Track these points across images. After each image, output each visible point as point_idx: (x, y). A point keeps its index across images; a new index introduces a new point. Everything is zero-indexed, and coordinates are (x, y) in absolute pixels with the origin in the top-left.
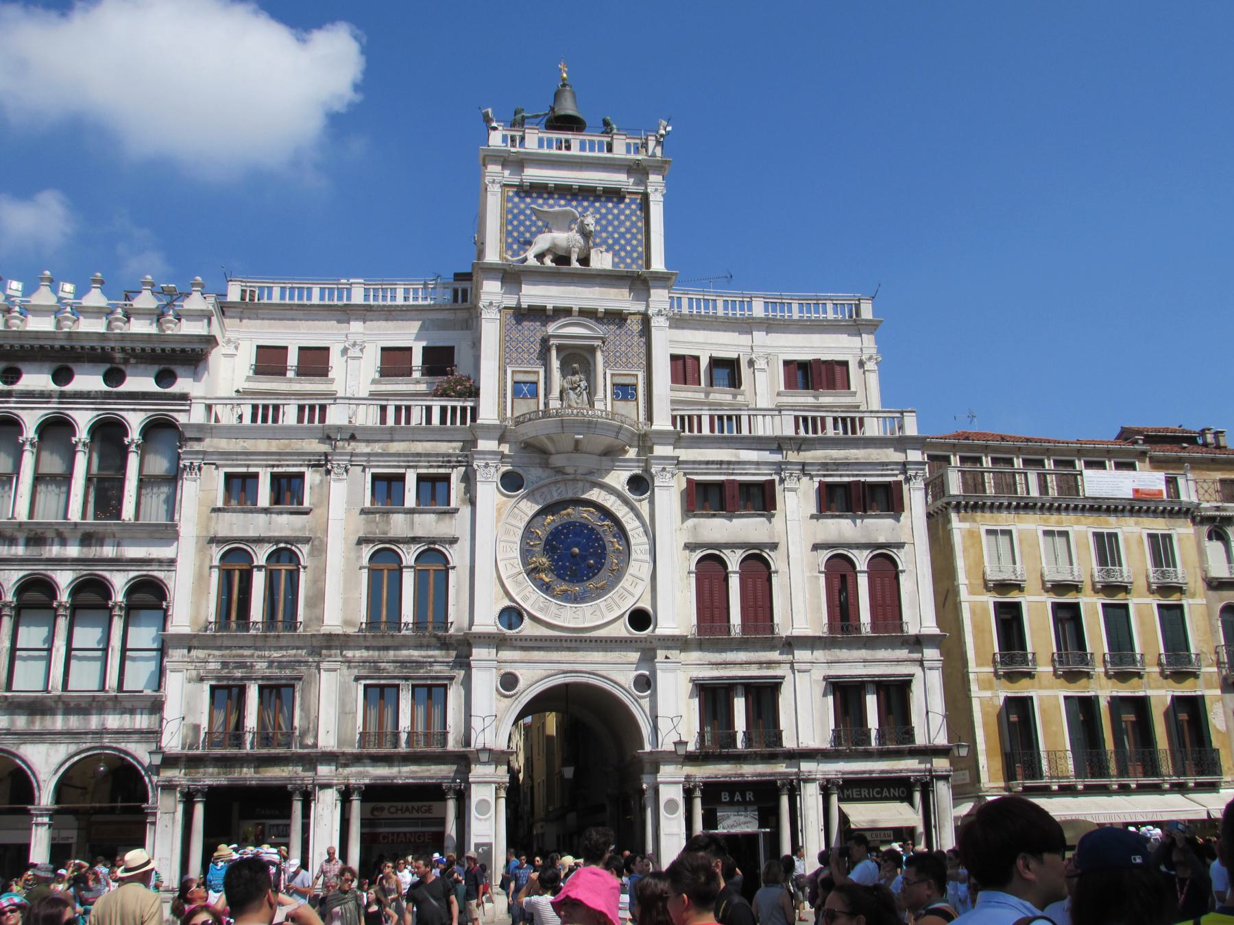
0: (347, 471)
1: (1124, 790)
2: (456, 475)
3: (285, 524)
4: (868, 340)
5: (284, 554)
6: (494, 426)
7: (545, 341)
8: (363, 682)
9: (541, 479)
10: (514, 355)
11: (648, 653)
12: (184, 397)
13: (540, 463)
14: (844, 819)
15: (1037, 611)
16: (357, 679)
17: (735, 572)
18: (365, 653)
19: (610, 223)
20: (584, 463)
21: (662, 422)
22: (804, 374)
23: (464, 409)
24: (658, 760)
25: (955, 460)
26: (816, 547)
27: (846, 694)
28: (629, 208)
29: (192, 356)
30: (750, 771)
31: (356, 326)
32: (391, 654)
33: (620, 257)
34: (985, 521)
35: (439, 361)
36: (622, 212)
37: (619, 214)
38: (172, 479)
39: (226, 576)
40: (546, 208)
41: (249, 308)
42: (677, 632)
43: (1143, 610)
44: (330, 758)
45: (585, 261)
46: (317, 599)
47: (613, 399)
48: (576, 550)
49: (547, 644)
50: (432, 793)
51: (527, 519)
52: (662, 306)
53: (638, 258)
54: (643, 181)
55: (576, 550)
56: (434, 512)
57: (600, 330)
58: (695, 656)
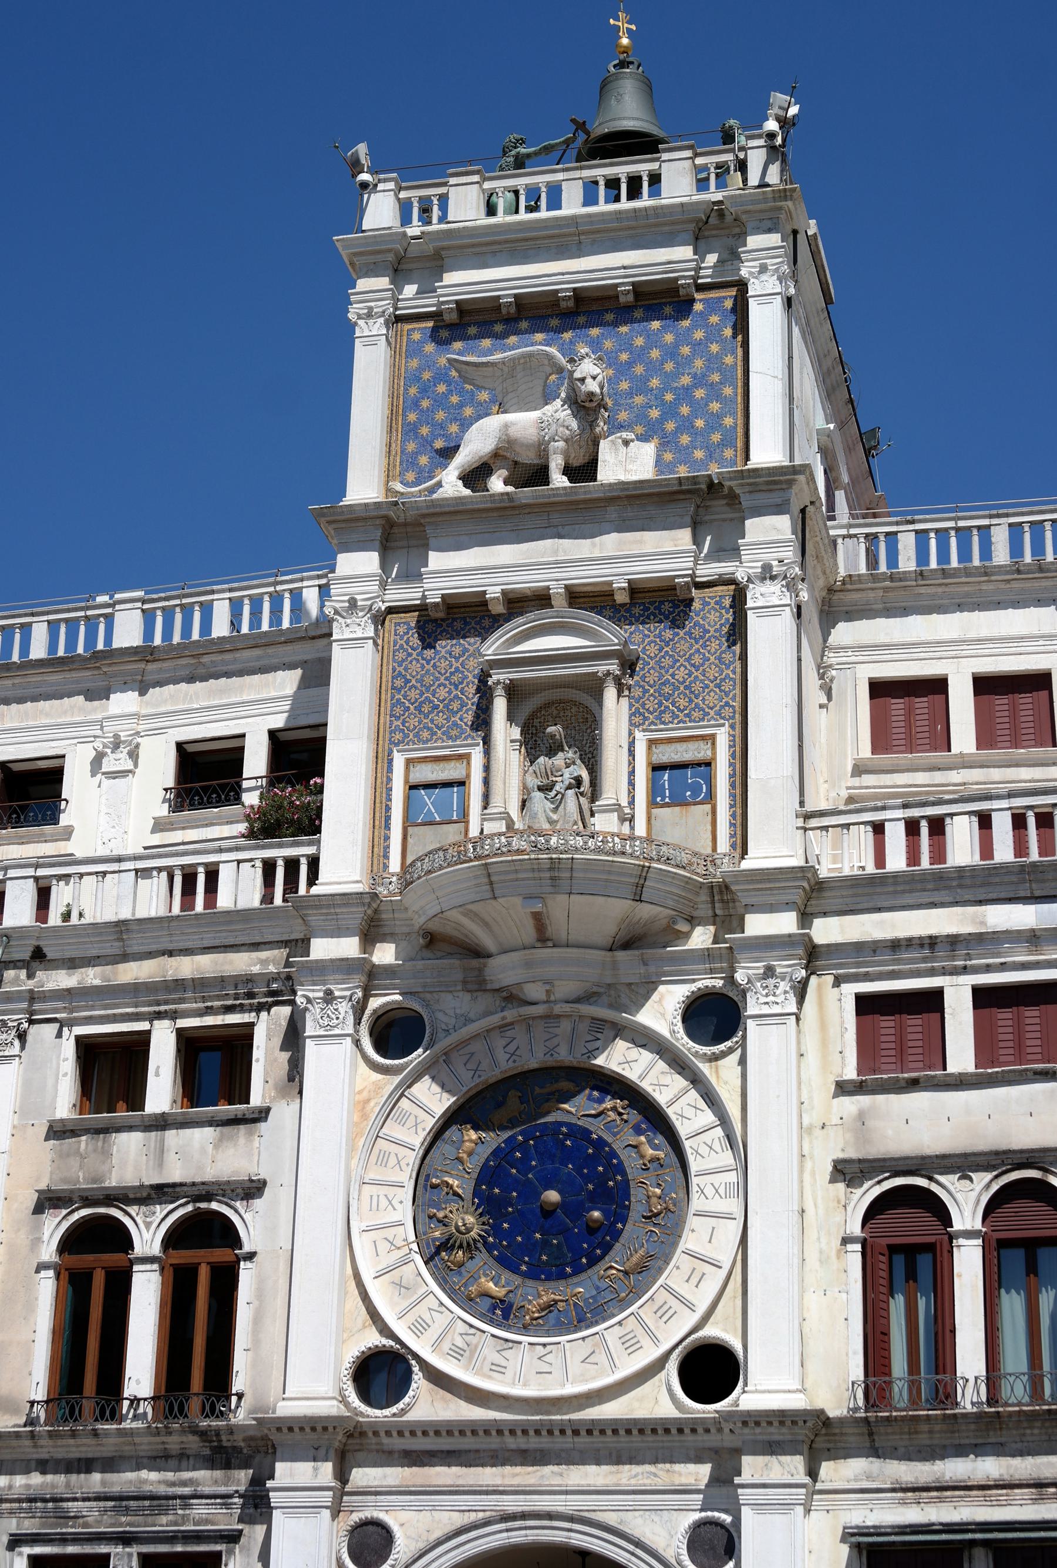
0: (22, 1036)
6: (345, 897)
8: (27, 1550)
9: (468, 1021)
10: (413, 722)
16: (15, 1542)
17: (969, 1234)
18: (36, 1479)
19: (654, 368)
23: (292, 865)
32: (96, 1480)
33: (679, 449)
36: (684, 338)
37: (676, 345)
40: (498, 356)
42: (796, 1402)
45: (583, 470)
47: (652, 804)
48: (552, 1196)
49: (468, 1443)
51: (430, 1123)
52: (770, 556)
53: (723, 444)
55: (552, 1196)
56: (212, 1122)
57: (611, 635)
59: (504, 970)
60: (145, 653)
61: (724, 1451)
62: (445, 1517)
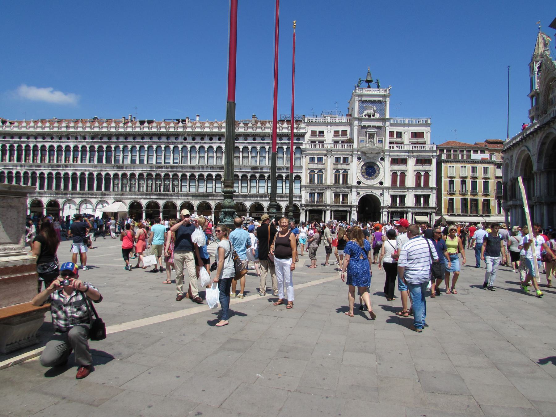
1: (470, 216)
3: (320, 166)
4: (429, 128)
5: (320, 171)
7: (366, 132)
12: (302, 143)
14: (415, 219)
15: (457, 182)
21: (387, 148)
22: (415, 135)
25: (445, 151)
26: (414, 171)
27: (418, 198)
30: (399, 210)
35: (344, 133)
38: (300, 158)
39: (310, 175)
43: (480, 183)
44: (329, 205)
45: (374, 116)
46: (326, 179)
50: (346, 211)
54: (386, 99)
57: (376, 130)
60: (331, 123)
61: (383, 189)
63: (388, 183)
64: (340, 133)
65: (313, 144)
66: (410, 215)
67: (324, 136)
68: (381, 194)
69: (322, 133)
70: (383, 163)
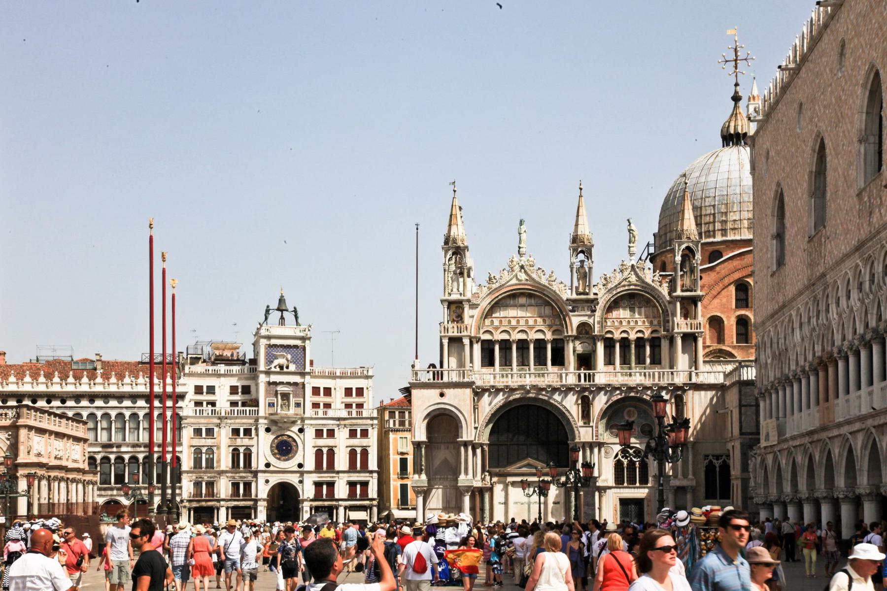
2: (253, 428)
3: (209, 442)
5: (210, 450)
7: (277, 391)
11: (302, 474)
13: (274, 425)
20: (286, 425)
24: (303, 501)
27: (352, 485)
28: (300, 351)
29: (182, 396)
30: (326, 503)
31: (222, 379)
34: (400, 435)
35: (246, 390)
41: (191, 375)
45: (287, 367)
46: (219, 461)
50: (249, 507)
58: (314, 475)
59: (280, 425)
62: (275, 479)
63: (310, 465)
64: (240, 390)
65: (198, 409)
66: (341, 511)
67: (214, 393)
68: (301, 482)
69: (211, 390)
70: (302, 436)
